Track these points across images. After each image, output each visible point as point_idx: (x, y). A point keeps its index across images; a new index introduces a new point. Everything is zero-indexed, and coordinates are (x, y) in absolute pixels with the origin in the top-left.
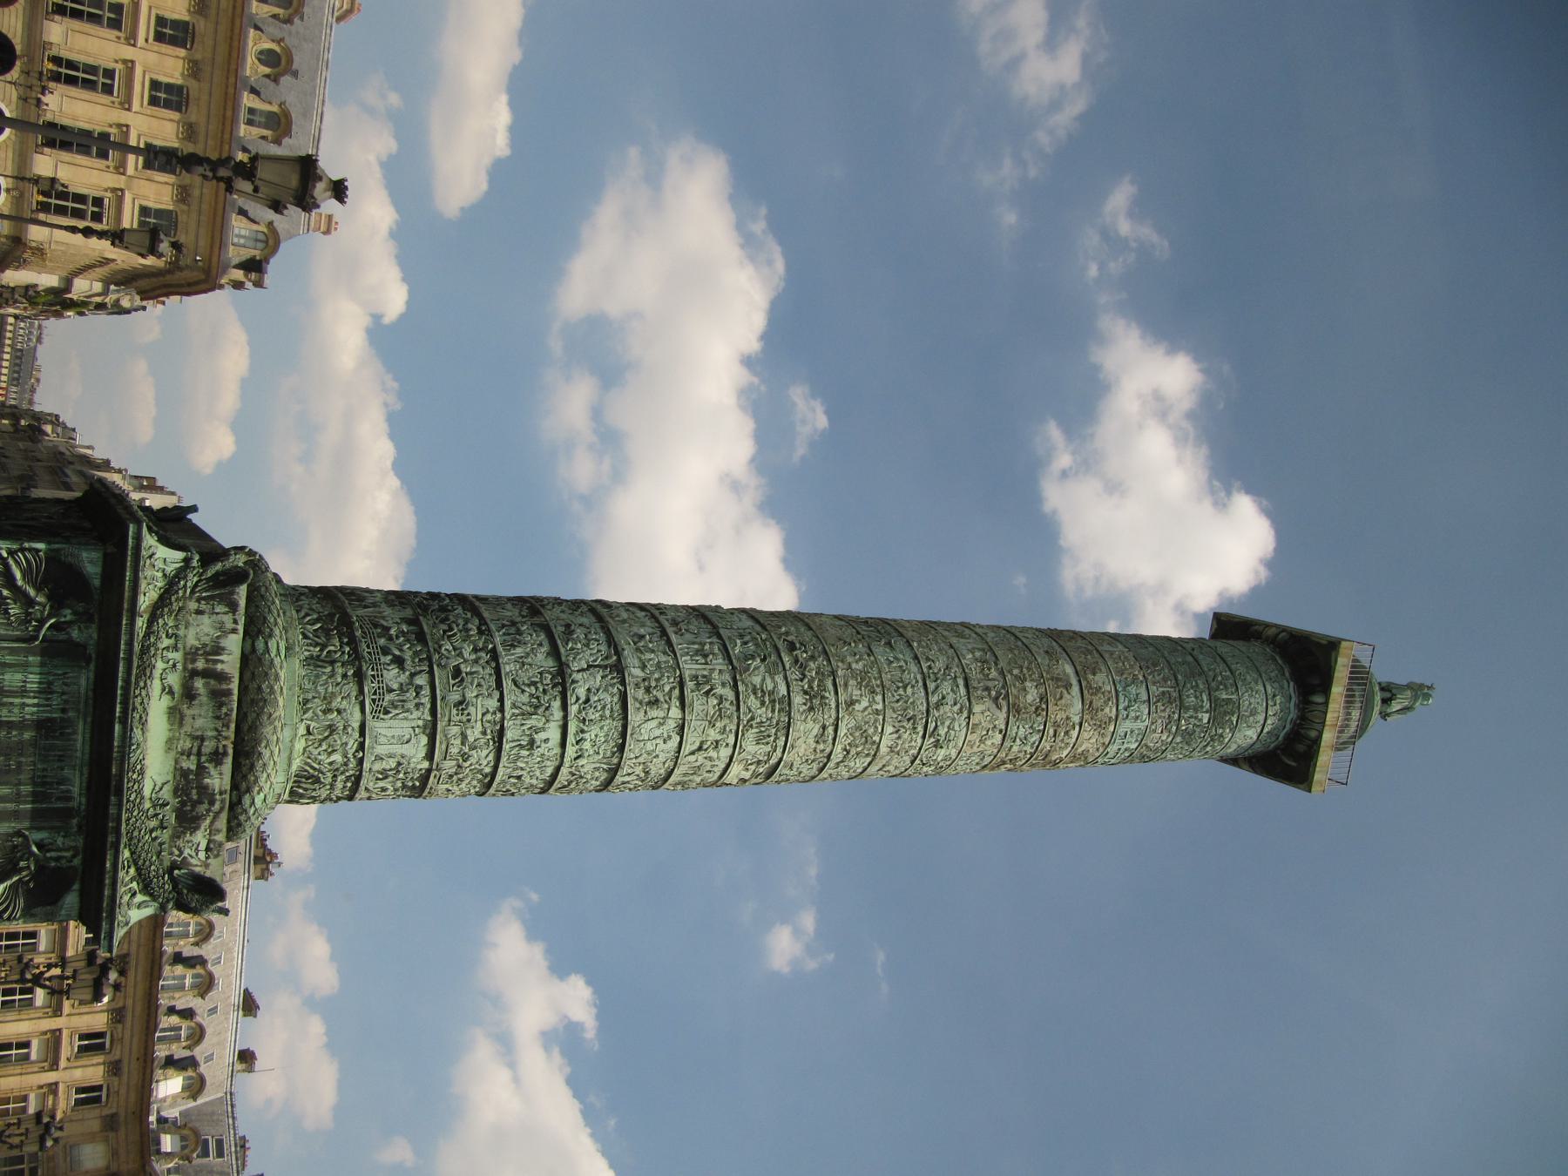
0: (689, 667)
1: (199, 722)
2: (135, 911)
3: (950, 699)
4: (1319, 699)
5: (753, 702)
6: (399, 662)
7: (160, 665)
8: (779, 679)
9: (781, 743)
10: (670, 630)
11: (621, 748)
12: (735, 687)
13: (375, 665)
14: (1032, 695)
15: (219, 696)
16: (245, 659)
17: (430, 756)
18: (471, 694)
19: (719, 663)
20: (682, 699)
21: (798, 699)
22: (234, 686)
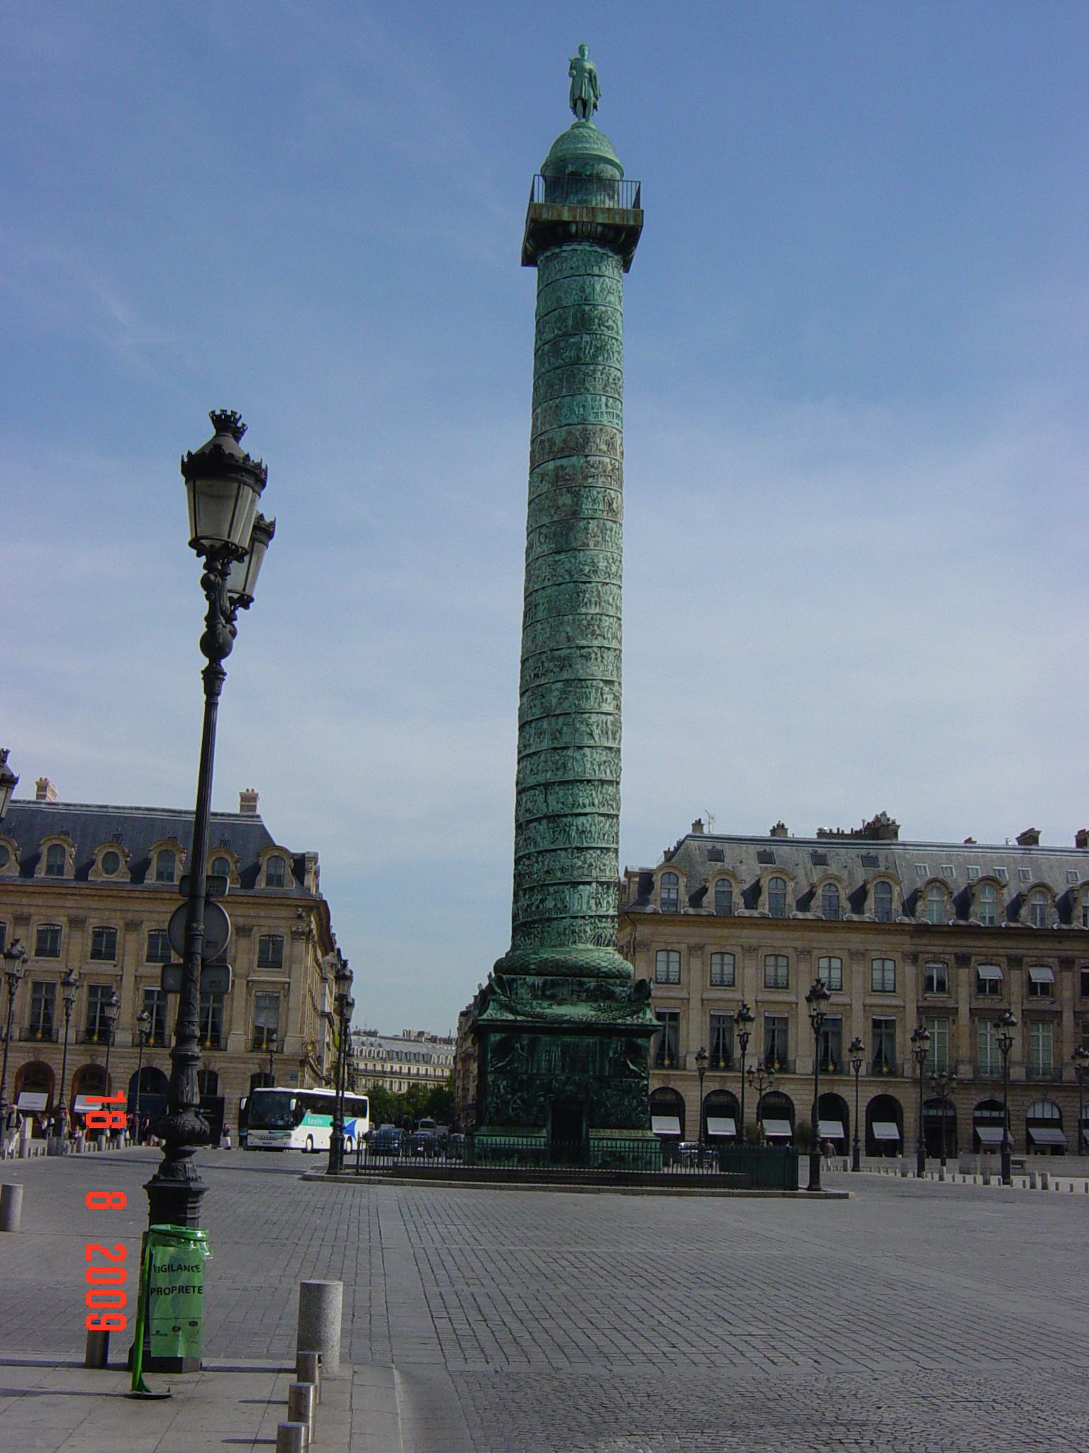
2: (649, 1016)
3: (568, 566)
4: (573, 228)
5: (566, 705)
6: (542, 901)
8: (554, 687)
10: (528, 751)
11: (589, 781)
12: (558, 716)
14: (566, 499)
15: (554, 984)
16: (538, 974)
17: (589, 883)
18: (558, 865)
19: (545, 724)
21: (565, 675)
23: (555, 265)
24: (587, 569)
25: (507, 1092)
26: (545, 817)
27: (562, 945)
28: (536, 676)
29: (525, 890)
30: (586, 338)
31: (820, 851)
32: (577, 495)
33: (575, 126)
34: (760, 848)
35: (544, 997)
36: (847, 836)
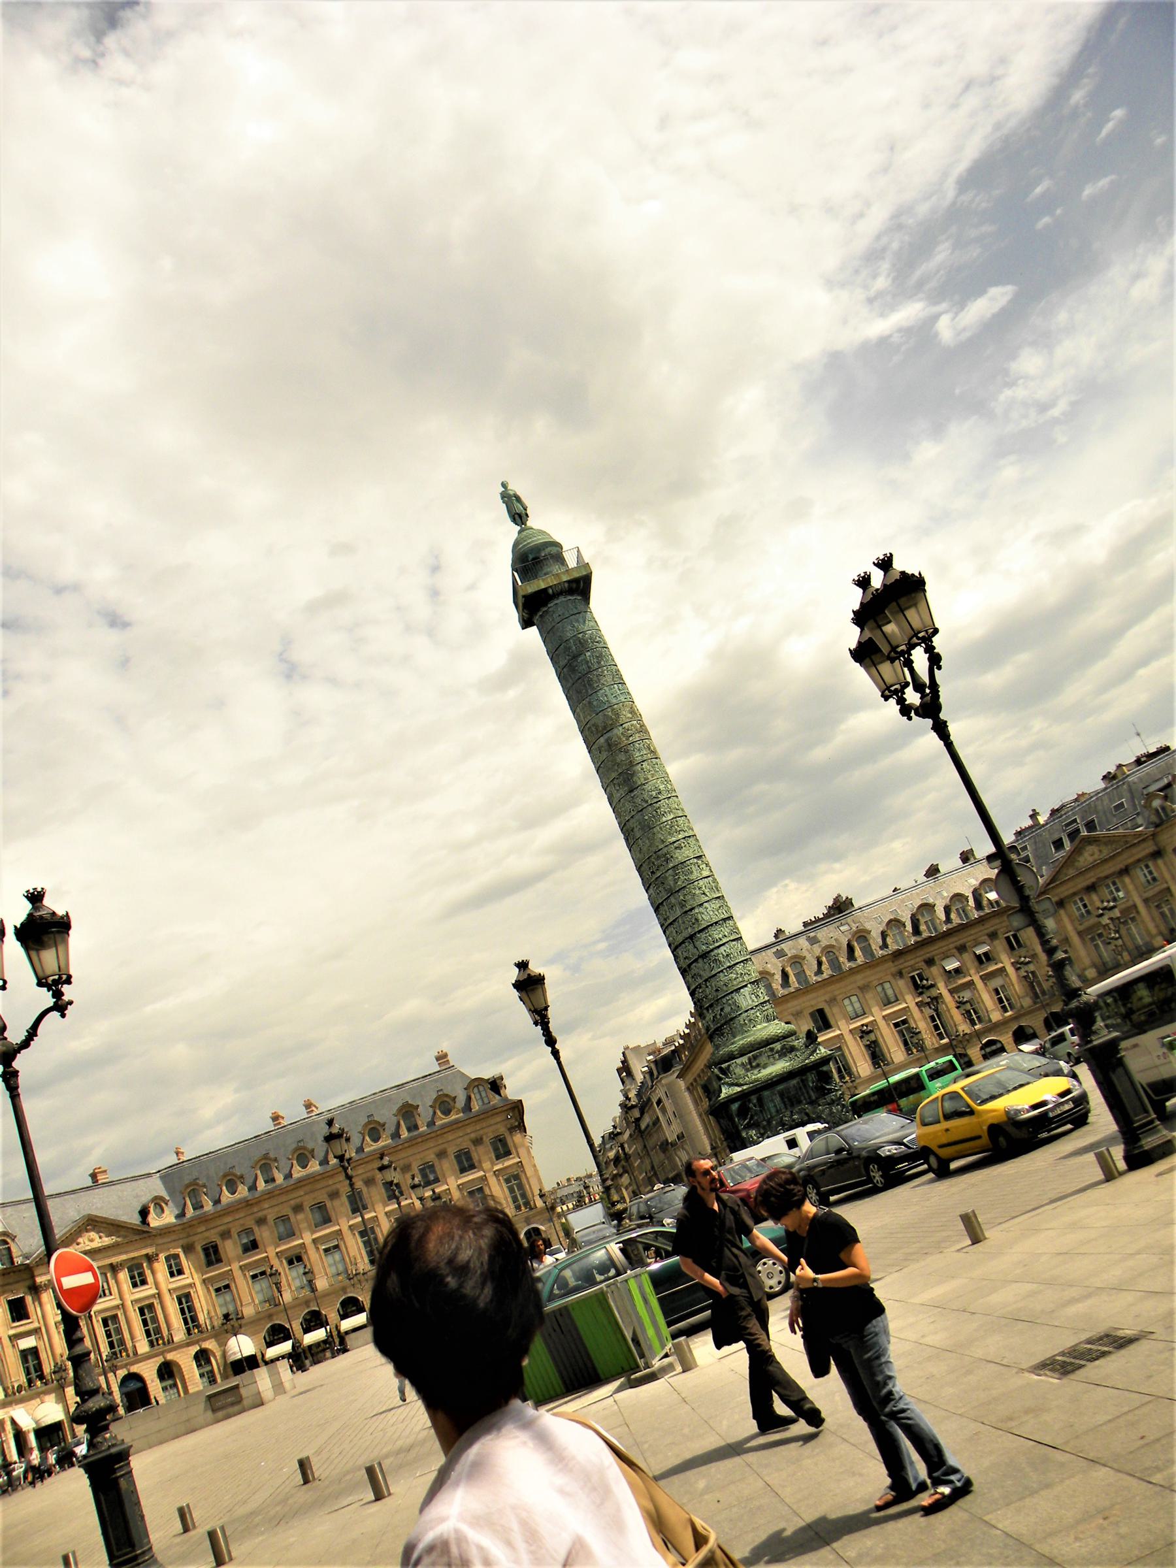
2: (823, 1051)
4: (550, 591)
6: (722, 1010)
10: (669, 922)
13: (726, 1016)
15: (755, 1057)
16: (742, 1055)
19: (672, 900)
20: (691, 910)
23: (548, 618)
24: (654, 793)
26: (700, 957)
28: (653, 873)
29: (707, 1009)
30: (588, 654)
31: (812, 935)
32: (627, 752)
33: (520, 532)
34: (774, 950)
35: (753, 1068)
36: (822, 919)
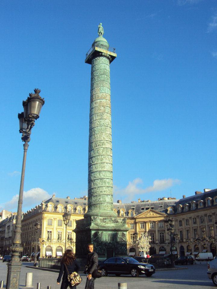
0: (100, 161)
1: (108, 221)
3: (103, 122)
4: (103, 54)
5: (104, 153)
6: (100, 199)
7: (103, 225)
9: (108, 149)
10: (94, 163)
11: (109, 171)
14: (102, 108)
15: (105, 219)
16: (101, 216)
17: (110, 195)
18: (103, 190)
21: (103, 146)
22: (104, 217)
25: (96, 246)
27: (105, 210)
30: (106, 76)
